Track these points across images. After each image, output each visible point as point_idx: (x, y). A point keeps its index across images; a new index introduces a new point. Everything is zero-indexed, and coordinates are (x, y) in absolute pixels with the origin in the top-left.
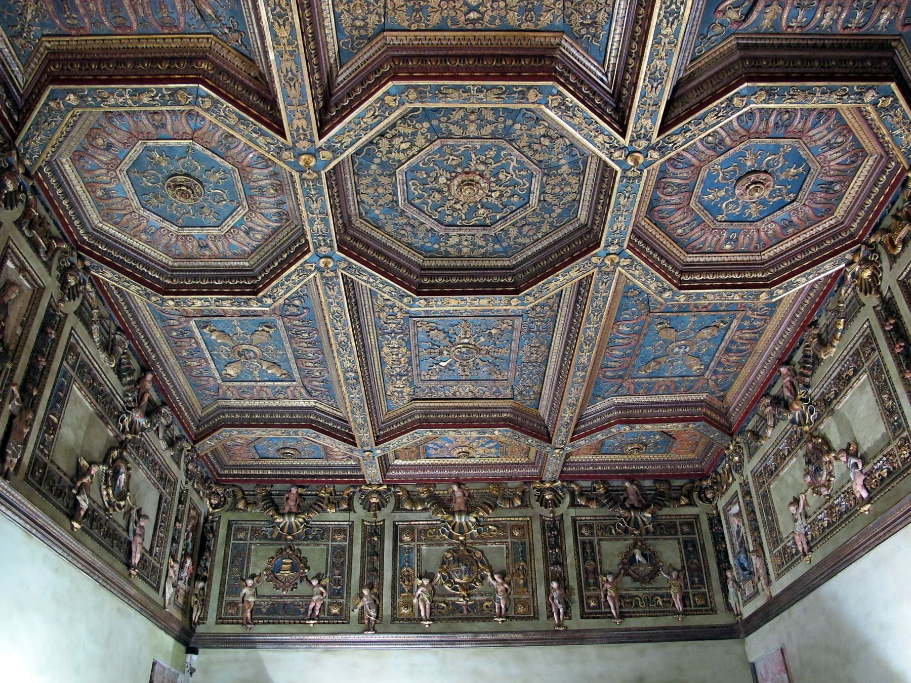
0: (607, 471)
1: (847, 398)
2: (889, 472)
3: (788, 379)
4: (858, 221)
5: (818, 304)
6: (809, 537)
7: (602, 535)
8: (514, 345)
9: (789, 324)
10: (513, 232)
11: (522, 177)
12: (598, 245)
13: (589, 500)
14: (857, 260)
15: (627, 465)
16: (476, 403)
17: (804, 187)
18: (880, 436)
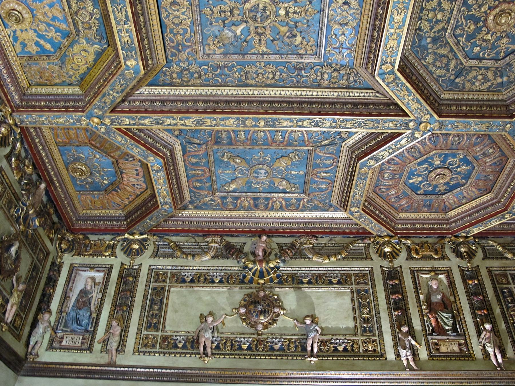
0: (43, 161)
1: (320, 290)
2: (345, 349)
3: (264, 245)
4: (405, 227)
5: (331, 233)
6: (214, 345)
7: (5, 205)
8: (273, 58)
9: (298, 223)
10: (443, 51)
11: (498, 53)
12: (440, 116)
13: (18, 168)
14: (386, 239)
15: (55, 174)
16: (157, 27)
17: (428, 196)
18: (344, 326)
